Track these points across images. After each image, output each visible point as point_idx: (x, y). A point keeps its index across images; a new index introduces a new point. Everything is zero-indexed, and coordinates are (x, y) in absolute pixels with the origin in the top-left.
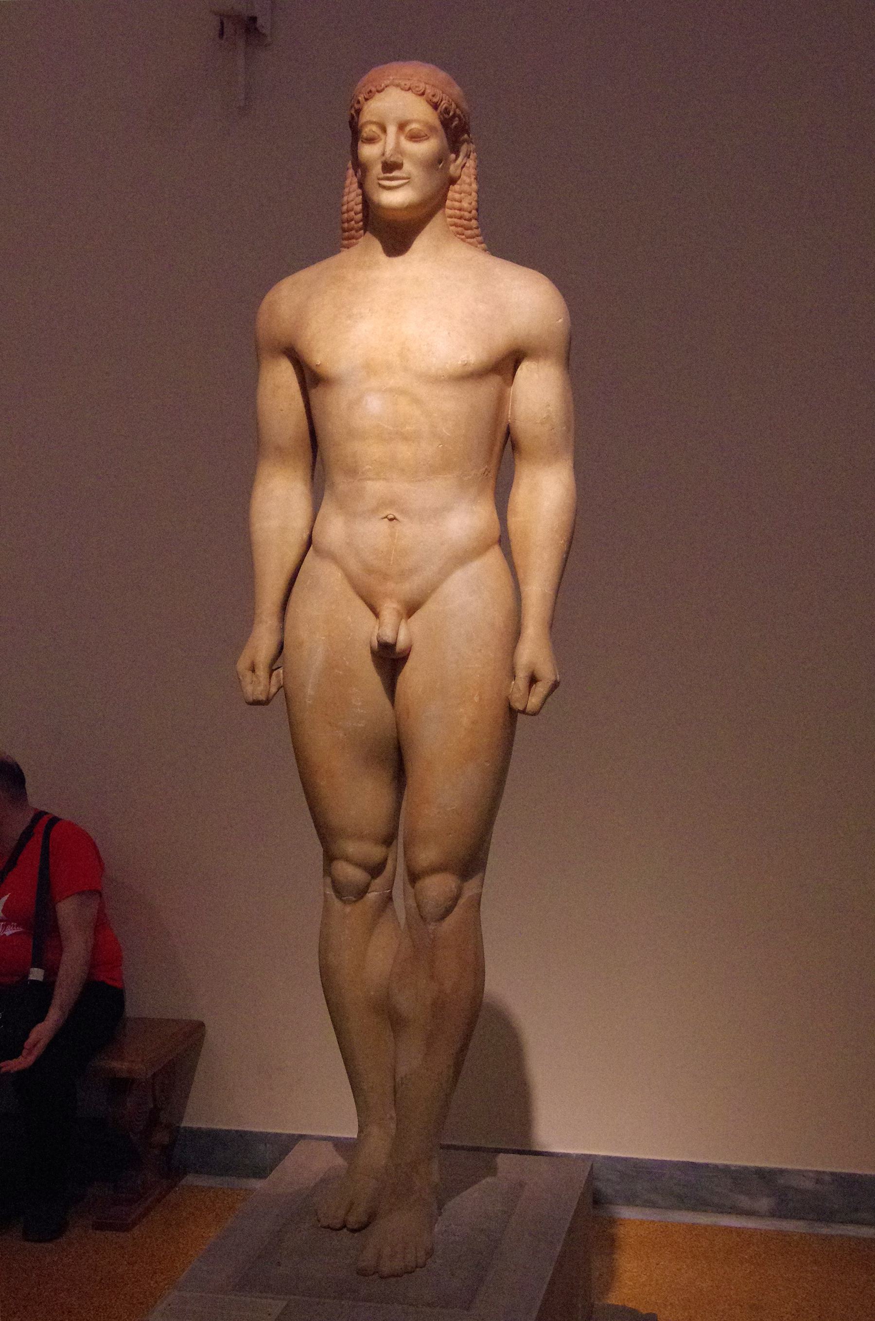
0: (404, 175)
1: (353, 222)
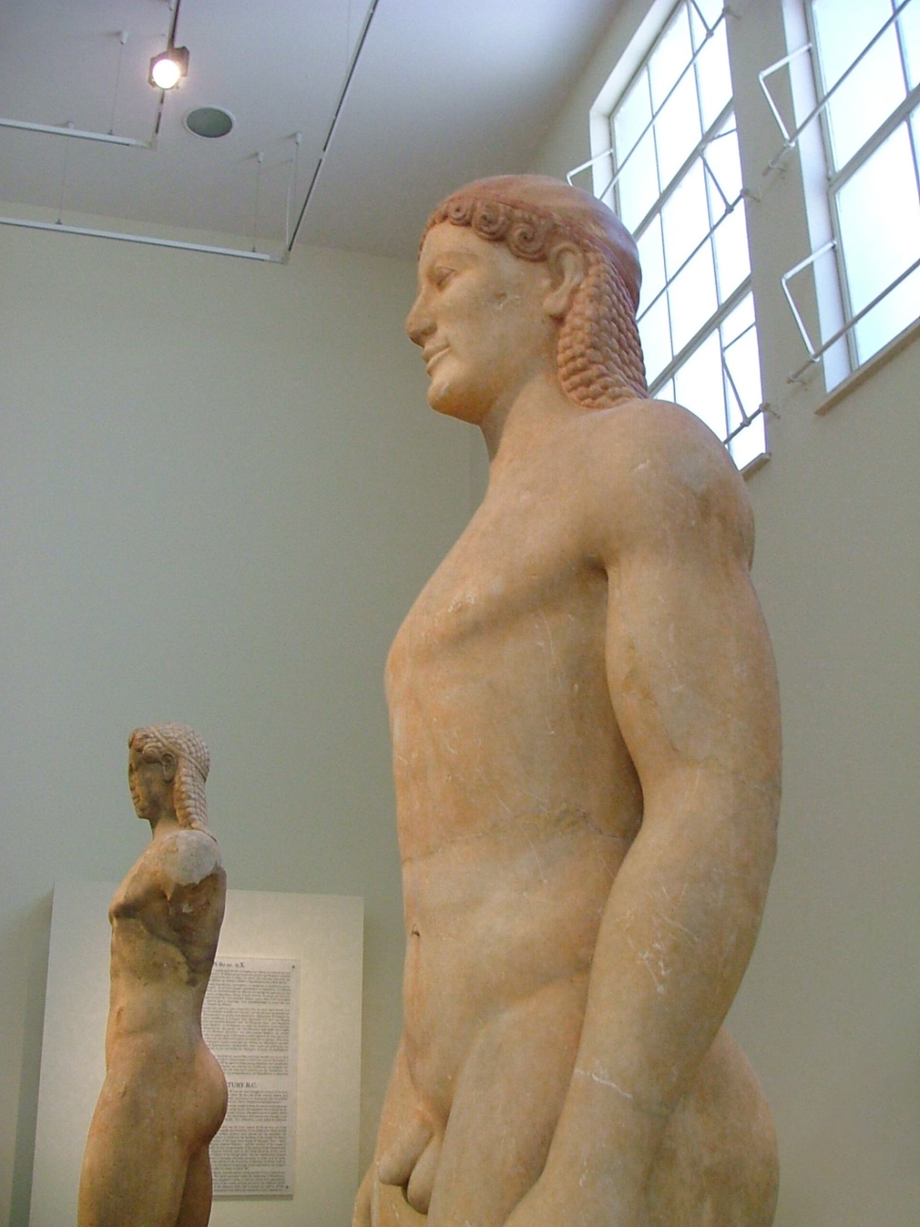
0: (438, 344)
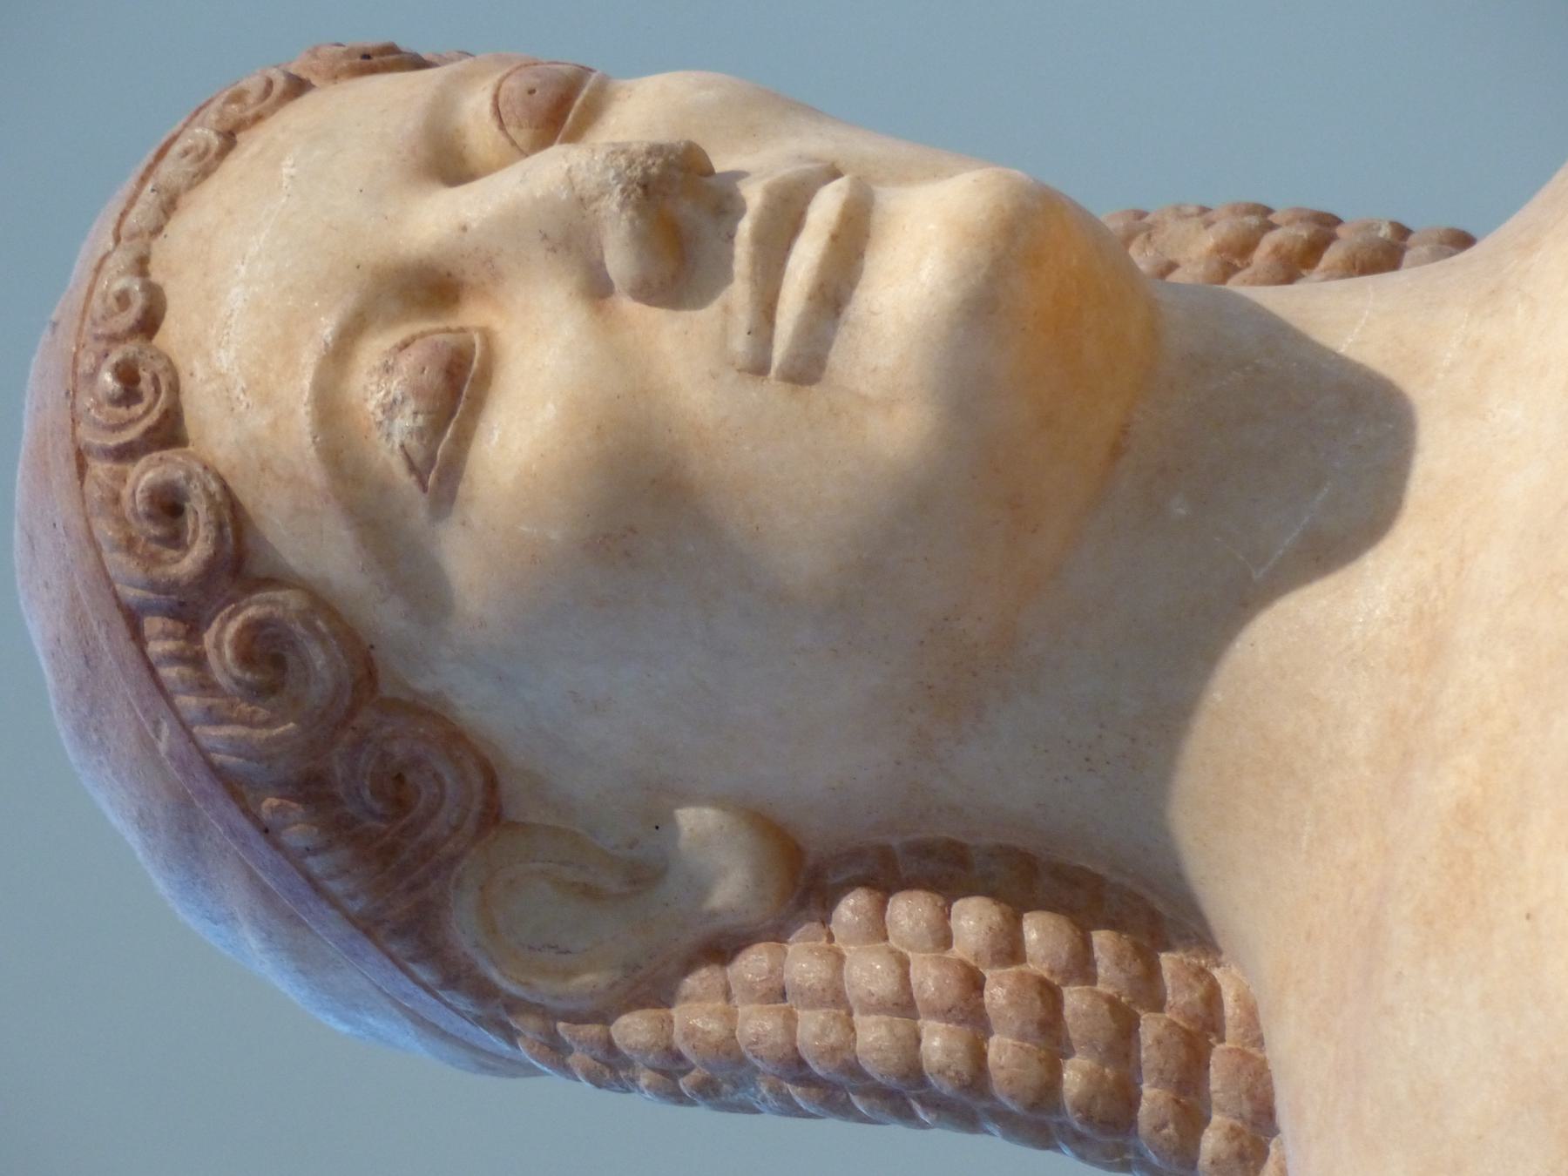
1: (1074, 999)
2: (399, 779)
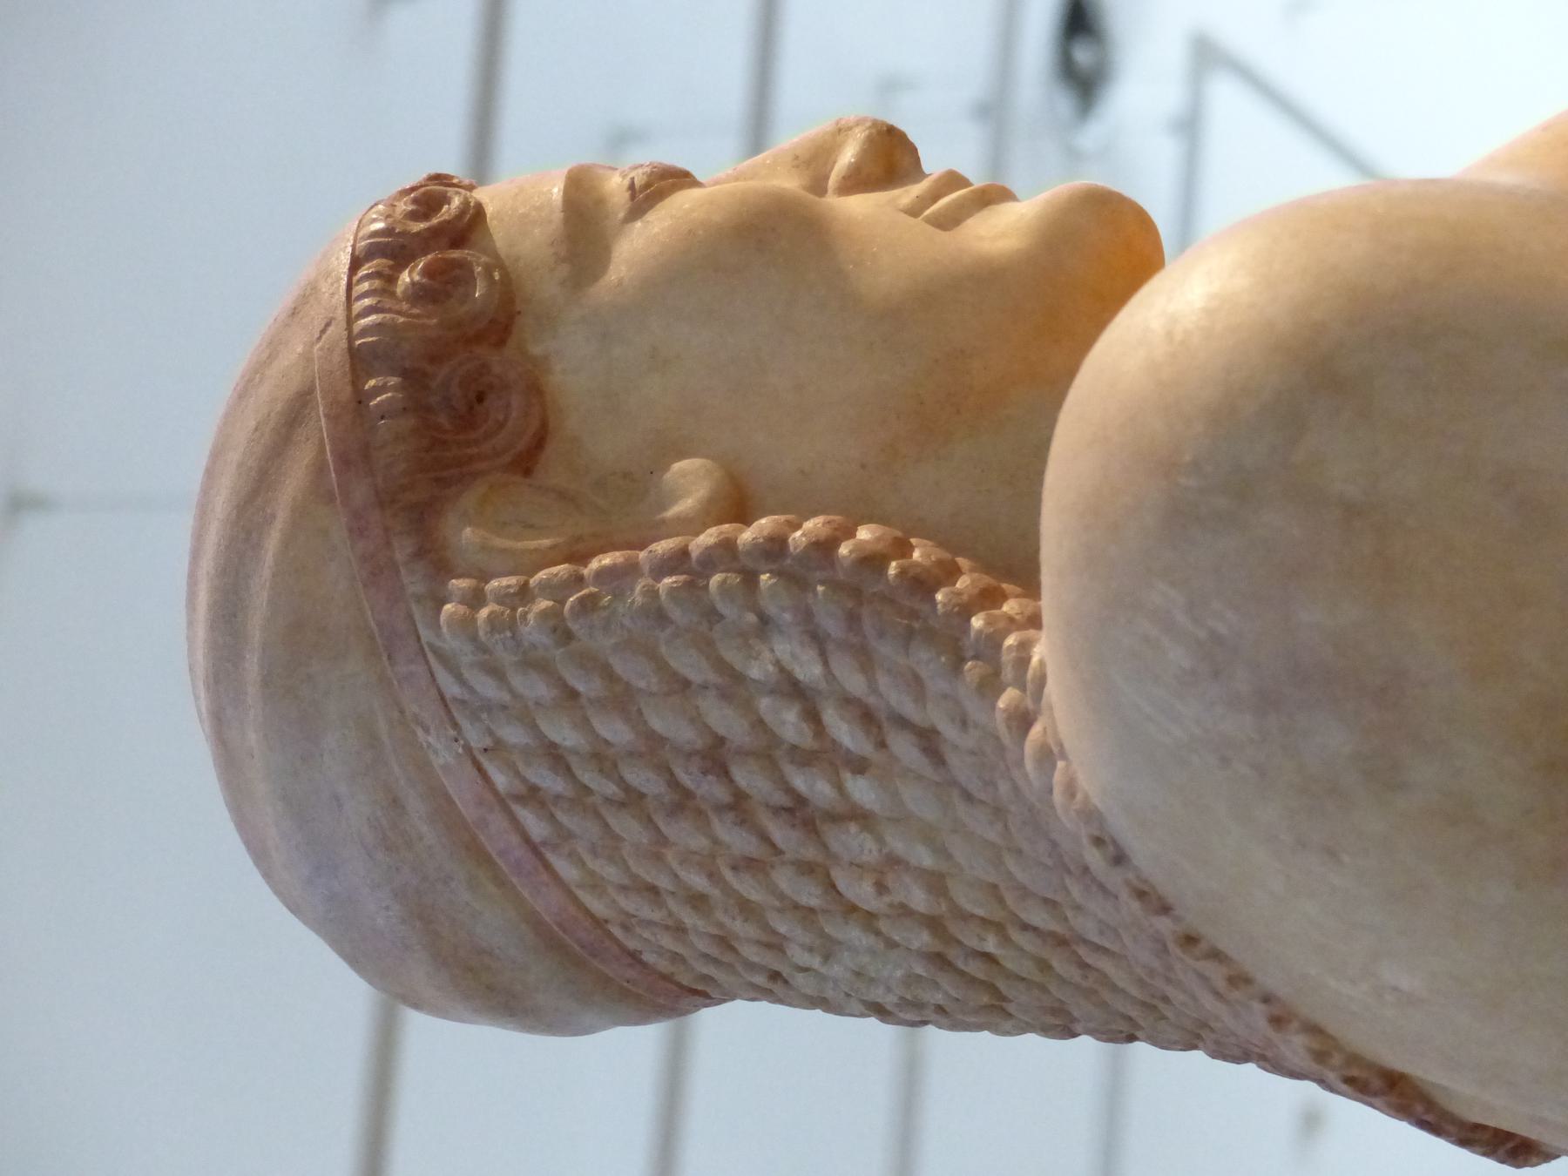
2: (480, 398)
